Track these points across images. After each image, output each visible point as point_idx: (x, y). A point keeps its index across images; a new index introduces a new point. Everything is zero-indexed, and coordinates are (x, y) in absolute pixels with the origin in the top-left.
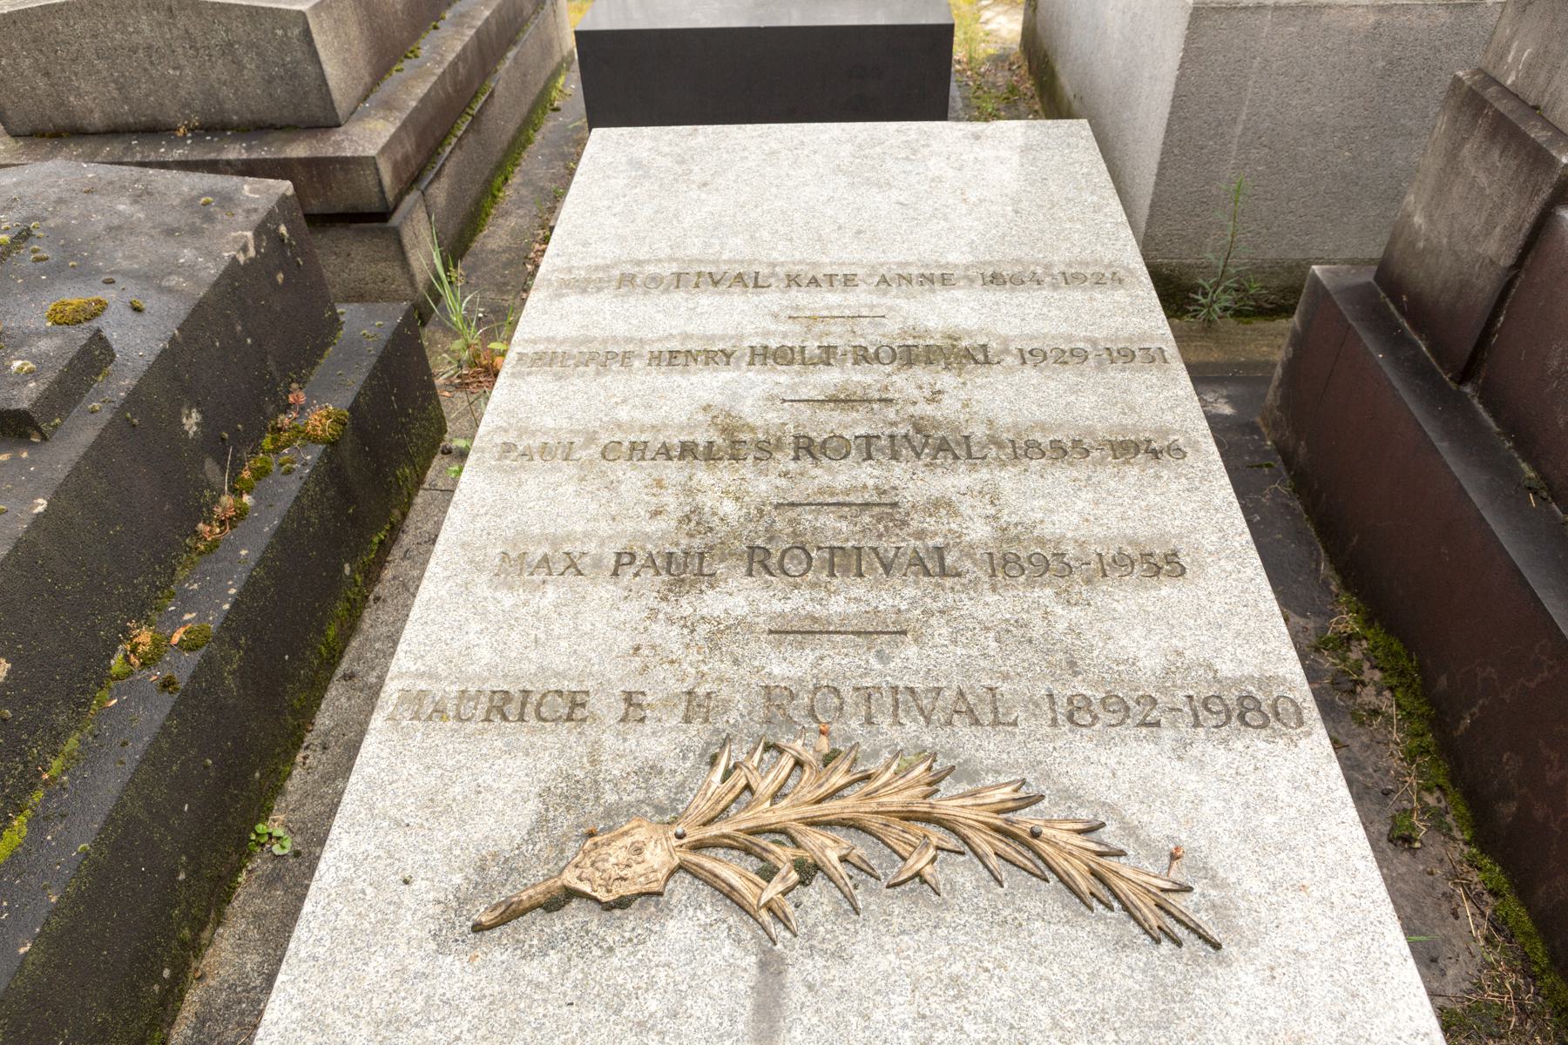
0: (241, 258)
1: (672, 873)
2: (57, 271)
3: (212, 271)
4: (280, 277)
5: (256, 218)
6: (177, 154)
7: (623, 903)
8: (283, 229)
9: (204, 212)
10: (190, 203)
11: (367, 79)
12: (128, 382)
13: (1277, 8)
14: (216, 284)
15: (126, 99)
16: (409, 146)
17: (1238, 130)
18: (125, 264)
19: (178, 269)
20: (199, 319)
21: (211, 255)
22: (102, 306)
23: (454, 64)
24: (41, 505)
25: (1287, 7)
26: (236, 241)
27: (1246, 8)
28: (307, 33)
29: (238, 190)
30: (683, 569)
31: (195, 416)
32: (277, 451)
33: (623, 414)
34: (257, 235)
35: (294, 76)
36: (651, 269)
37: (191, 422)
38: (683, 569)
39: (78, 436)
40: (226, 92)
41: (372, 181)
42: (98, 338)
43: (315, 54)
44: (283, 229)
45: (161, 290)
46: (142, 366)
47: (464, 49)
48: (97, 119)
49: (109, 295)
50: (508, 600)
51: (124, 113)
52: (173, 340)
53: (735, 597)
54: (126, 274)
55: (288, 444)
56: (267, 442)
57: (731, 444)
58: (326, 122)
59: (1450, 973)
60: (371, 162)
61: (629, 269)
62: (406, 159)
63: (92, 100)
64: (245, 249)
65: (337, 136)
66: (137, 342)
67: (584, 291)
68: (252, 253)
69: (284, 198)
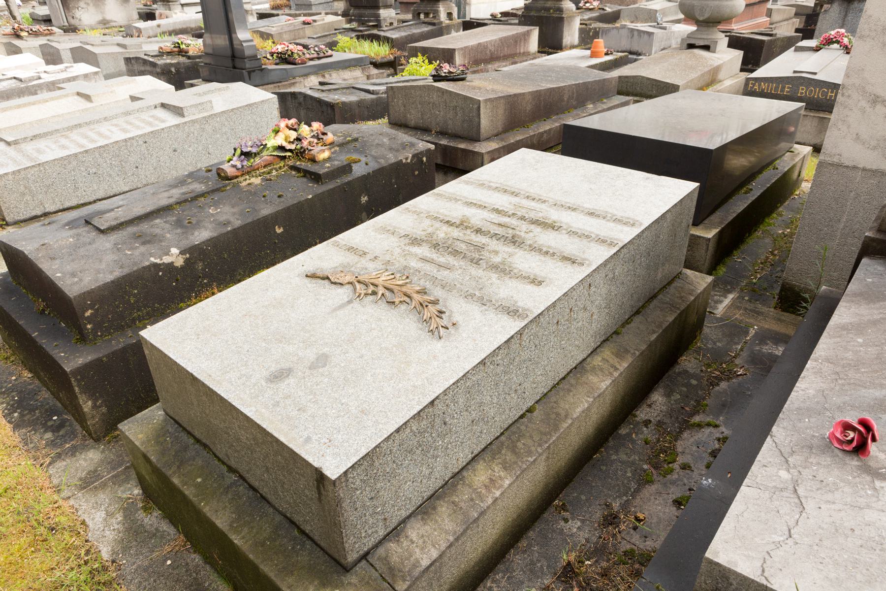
0: (404, 161)
1: (349, 283)
2: (356, 150)
4: (417, 173)
6: (428, 138)
7: (335, 283)
8: (424, 159)
9: (404, 146)
11: (500, 129)
12: (350, 179)
13: (864, 169)
14: (392, 164)
15: (422, 119)
17: (841, 226)
18: (373, 153)
19: (384, 157)
20: (381, 171)
21: (396, 157)
22: (359, 161)
23: (542, 134)
24: (310, 197)
25: (870, 170)
26: (407, 156)
27: (847, 167)
28: (479, 107)
30: (415, 241)
31: (366, 198)
33: (441, 211)
34: (413, 156)
35: (471, 121)
37: (364, 199)
38: (415, 241)
39: (331, 186)
40: (450, 122)
42: (350, 167)
43: (479, 115)
44: (424, 159)
46: (356, 176)
47: (550, 130)
48: (412, 123)
49: (363, 159)
50: (373, 233)
51: (420, 123)
52: (369, 174)
53: (424, 251)
54: (372, 156)
57: (463, 224)
58: (476, 139)
59: (647, 543)
61: (486, 182)
63: (413, 117)
64: (407, 159)
65: (477, 144)
66: (359, 170)
68: (409, 161)
69: (429, 150)
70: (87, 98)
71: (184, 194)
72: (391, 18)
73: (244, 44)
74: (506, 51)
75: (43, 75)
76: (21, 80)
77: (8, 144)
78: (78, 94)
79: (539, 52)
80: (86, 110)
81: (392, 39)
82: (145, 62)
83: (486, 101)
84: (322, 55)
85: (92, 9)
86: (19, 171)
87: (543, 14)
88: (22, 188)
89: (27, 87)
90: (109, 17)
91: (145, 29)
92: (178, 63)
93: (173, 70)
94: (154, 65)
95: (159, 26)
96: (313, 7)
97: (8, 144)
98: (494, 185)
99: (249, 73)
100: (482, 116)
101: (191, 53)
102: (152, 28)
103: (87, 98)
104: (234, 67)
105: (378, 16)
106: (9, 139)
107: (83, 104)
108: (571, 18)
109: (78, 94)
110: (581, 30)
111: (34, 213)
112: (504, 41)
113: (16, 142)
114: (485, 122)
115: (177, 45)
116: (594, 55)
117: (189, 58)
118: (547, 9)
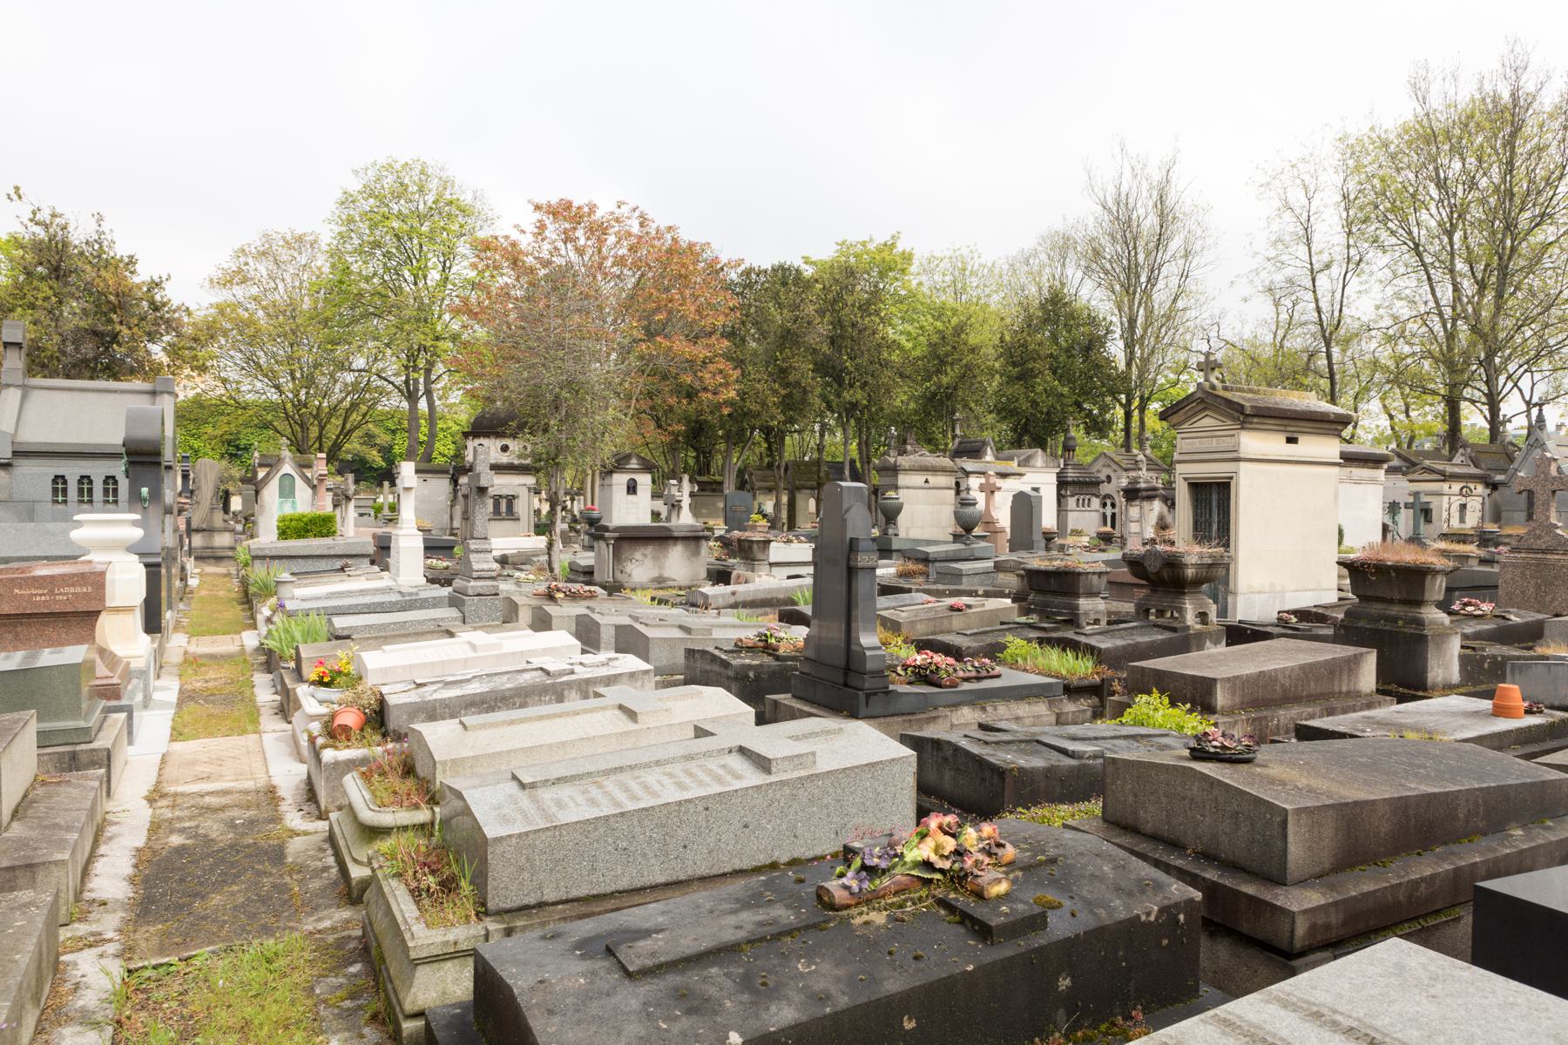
0: (1143, 918)
2: (1053, 882)
3: (1122, 915)
4: (1165, 942)
5: (1166, 902)
6: (1179, 863)
8: (1182, 917)
9: (1143, 887)
10: (1139, 881)
11: (1327, 866)
12: (1043, 942)
14: (1120, 923)
15: (1168, 823)
16: (1335, 919)
18: (1085, 893)
19: (1106, 906)
20: (1099, 934)
21: (1128, 908)
22: (1060, 906)
24: (970, 968)
26: (1148, 909)
28: (1285, 823)
29: (1170, 885)
31: (1068, 982)
32: (1105, 1034)
34: (1162, 910)
36: (1338, 1018)
37: (1064, 983)
39: (1005, 951)
40: (1224, 838)
41: (1287, 927)
42: (1043, 916)
43: (1285, 836)
44: (1182, 917)
45: (1091, 911)
46: (1054, 939)
47: (1433, 877)
48: (1149, 828)
49: (1067, 903)
51: (1164, 830)
52: (1077, 936)
54: (1083, 898)
55: (1114, 1035)
56: (1103, 1027)
58: (1278, 879)
60: (1291, 915)
61: (1325, 1011)
62: (1327, 927)
63: (1150, 817)
64: (1148, 914)
65: (1280, 891)
66: (1060, 926)
67: (1285, 1007)
68: (1152, 918)
69: (1191, 901)
70: (632, 715)
71: (761, 924)
72: (1097, 612)
73: (868, 653)
74: (1313, 688)
75: (578, 669)
76: (547, 673)
77: (523, 786)
78: (621, 707)
79: (1378, 691)
80: (627, 733)
81: (1100, 650)
82: (714, 658)
83: (1299, 811)
84: (984, 673)
85: (649, 562)
86: (527, 834)
87: (1382, 625)
88: (523, 860)
89: (553, 685)
90: (667, 574)
91: (716, 596)
92: (761, 666)
93: (751, 674)
94: (726, 664)
95: (734, 593)
96: (964, 579)
97: (523, 786)
98: (1346, 1022)
99: (868, 696)
100: (1291, 838)
101: (781, 652)
102: (723, 595)
103: (632, 715)
104: (846, 685)
105: (1077, 607)
106: (526, 780)
107: (625, 724)
108: (1443, 636)
109: (621, 707)
110: (1462, 658)
111: (525, 902)
112: (1308, 671)
113: (533, 786)
114: (1297, 850)
115: (764, 638)
116: (1499, 712)
117: (778, 658)
118: (1395, 619)
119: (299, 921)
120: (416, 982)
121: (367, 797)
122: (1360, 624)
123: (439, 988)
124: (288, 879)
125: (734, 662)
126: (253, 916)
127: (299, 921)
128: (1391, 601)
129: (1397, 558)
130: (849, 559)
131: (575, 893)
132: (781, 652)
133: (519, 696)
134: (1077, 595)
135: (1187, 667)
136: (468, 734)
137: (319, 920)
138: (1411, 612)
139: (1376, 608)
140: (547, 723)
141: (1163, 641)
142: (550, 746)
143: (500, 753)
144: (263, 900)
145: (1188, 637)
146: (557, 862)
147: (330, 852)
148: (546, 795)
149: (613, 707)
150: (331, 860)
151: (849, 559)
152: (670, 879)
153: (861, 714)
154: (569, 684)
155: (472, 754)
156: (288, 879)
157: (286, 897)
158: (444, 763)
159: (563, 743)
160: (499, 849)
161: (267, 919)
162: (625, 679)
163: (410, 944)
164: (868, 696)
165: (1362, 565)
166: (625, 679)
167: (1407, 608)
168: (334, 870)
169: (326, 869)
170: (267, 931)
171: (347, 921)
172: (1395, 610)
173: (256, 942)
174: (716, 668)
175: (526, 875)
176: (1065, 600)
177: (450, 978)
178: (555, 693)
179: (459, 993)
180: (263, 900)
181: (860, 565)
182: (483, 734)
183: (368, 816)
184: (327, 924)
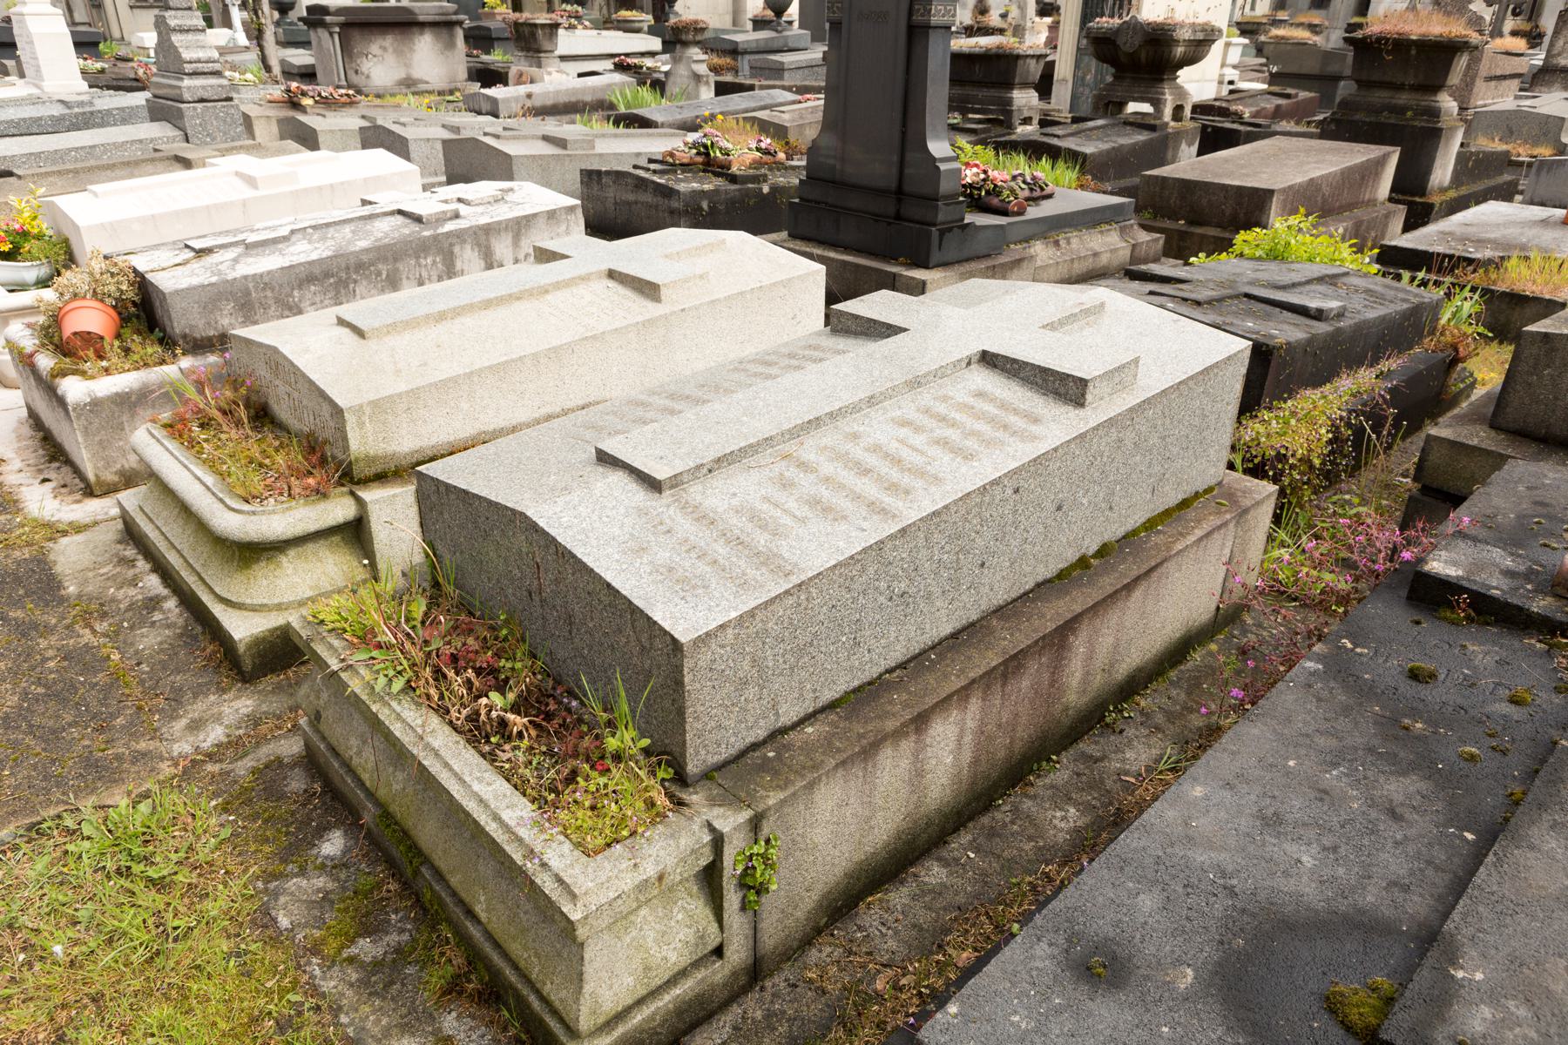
70: (648, 289)
72: (1030, 108)
73: (943, 167)
74: (1346, 197)
75: (463, 209)
76: (418, 219)
77: (653, 484)
78: (612, 274)
79: (1390, 200)
80: (650, 323)
81: (1085, 156)
82: (641, 184)
84: (1037, 193)
85: (390, 58)
86: (752, 614)
87: (1385, 117)
88: (746, 665)
89: (435, 238)
90: (417, 73)
91: (507, 100)
92: (716, 191)
93: (705, 205)
94: (667, 192)
95: (529, 96)
96: (786, 75)
97: (653, 484)
99: (942, 233)
101: (734, 169)
102: (517, 99)
103: (648, 289)
104: (898, 217)
105: (1009, 102)
106: (660, 473)
107: (638, 308)
108: (1453, 129)
109: (612, 274)
110: (1459, 154)
111: (750, 740)
112: (1347, 174)
113: (676, 481)
115: (704, 150)
117: (733, 179)
118: (1401, 110)
119: (155, 734)
120: (588, 969)
121: (210, 480)
122: (1357, 117)
123: (636, 964)
124: (87, 636)
125: (682, 187)
126: (52, 737)
127: (155, 734)
128: (1399, 88)
129: (1423, 30)
130: (910, 12)
131: (828, 695)
132: (734, 169)
133: (385, 260)
134: (1010, 86)
135: (1231, 175)
136: (372, 344)
137: (196, 726)
138: (1424, 100)
139: (1380, 96)
140: (501, 312)
141: (1145, 143)
142: (535, 356)
143: (454, 380)
144: (60, 694)
145: (1167, 136)
146: (801, 651)
147: (142, 564)
148: (715, 495)
149: (599, 275)
150: (153, 583)
151: (910, 12)
152: (958, 625)
153: (934, 259)
154: (459, 235)
155: (402, 387)
156: (87, 636)
157: (101, 678)
158: (359, 410)
159: (555, 350)
160: (704, 658)
161: (83, 739)
162: (542, 221)
163: (575, 916)
164: (942, 233)
165: (1379, 40)
166: (542, 221)
167: (1418, 96)
168: (171, 604)
169: (153, 603)
170: (98, 772)
171: (255, 721)
172: (1403, 98)
173: (87, 804)
174: (647, 197)
175: (751, 692)
176: (993, 93)
177: (651, 936)
178: (440, 251)
179: (673, 957)
180: (60, 694)
181: (934, 20)
182: (402, 342)
183: (232, 522)
184: (214, 735)
